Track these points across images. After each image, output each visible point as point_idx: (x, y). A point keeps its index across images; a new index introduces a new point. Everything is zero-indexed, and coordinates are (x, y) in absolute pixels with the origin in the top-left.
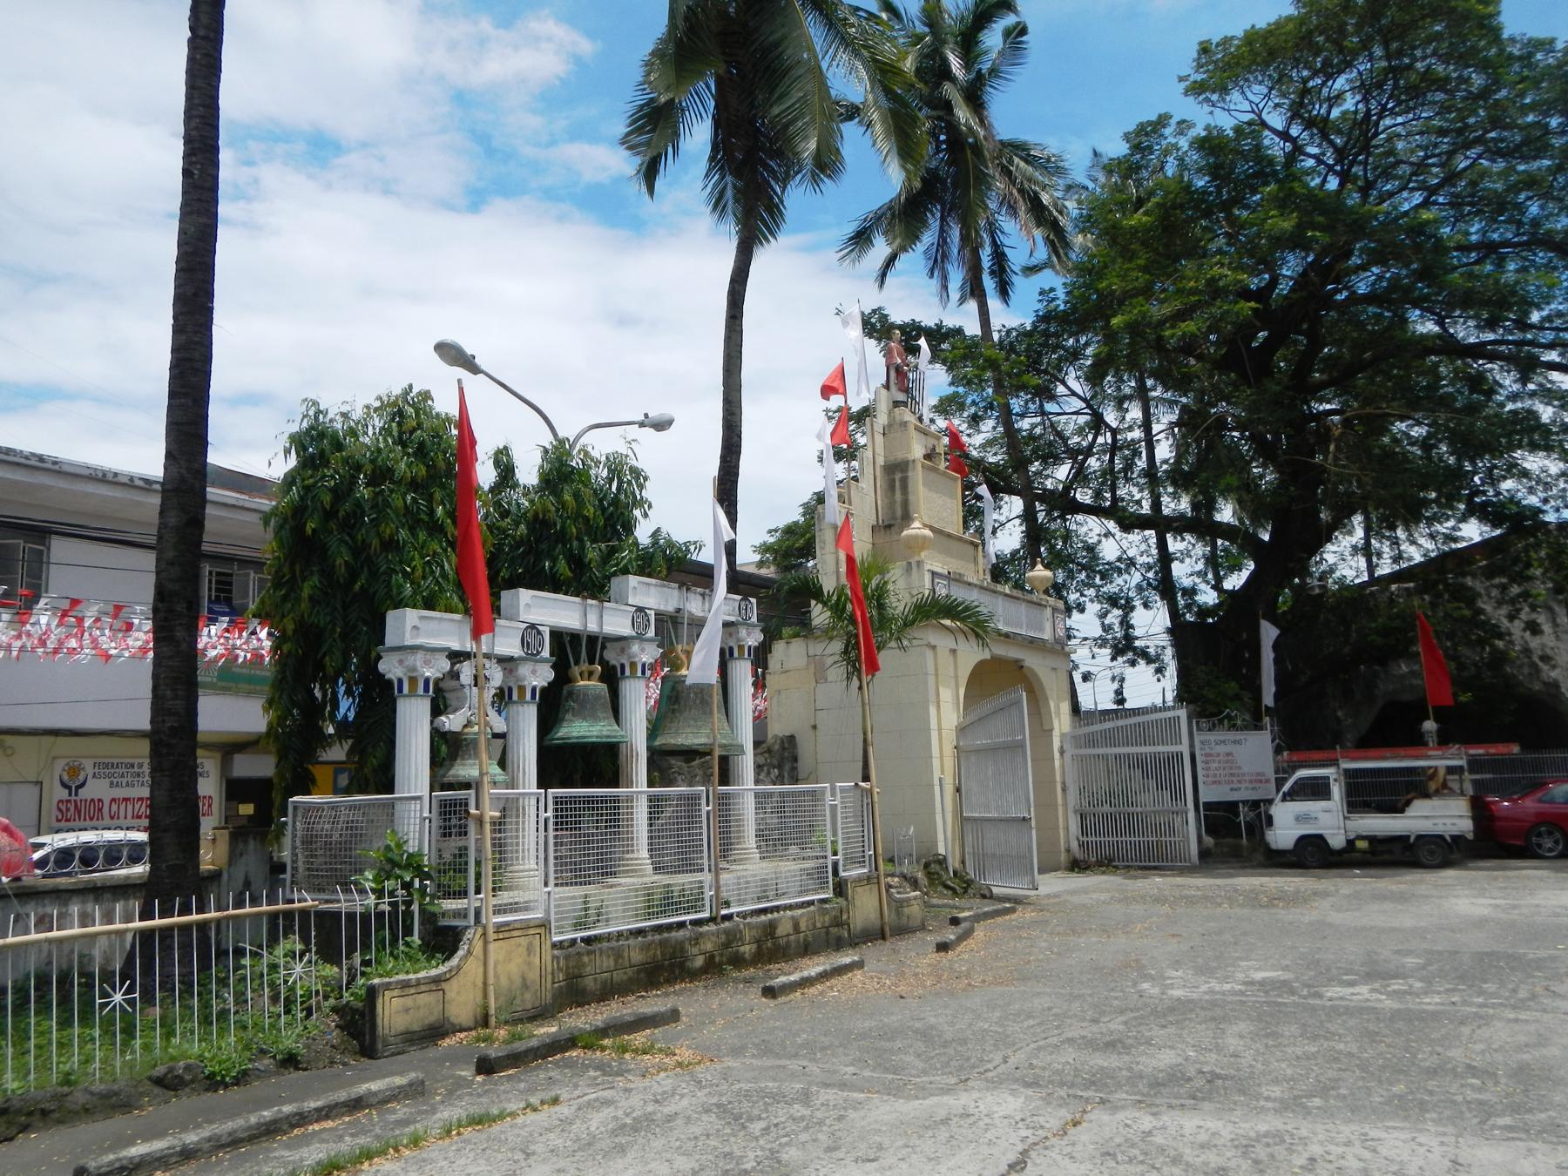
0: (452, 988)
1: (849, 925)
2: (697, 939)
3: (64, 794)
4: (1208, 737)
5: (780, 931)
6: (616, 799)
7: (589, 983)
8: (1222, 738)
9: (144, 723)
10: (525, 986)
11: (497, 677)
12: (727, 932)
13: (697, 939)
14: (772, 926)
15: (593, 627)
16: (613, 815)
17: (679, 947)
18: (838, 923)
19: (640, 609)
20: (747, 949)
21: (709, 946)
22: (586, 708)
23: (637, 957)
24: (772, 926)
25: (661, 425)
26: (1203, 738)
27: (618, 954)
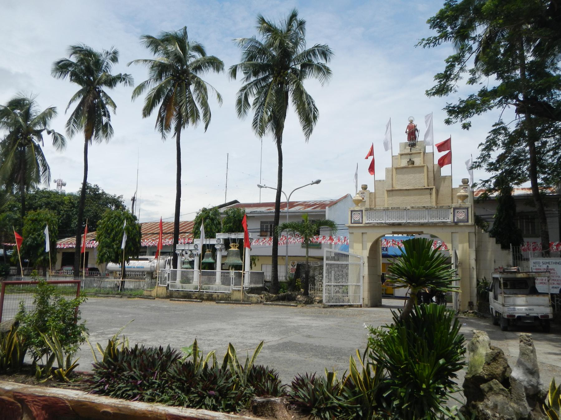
0: (152, 292)
1: (231, 298)
2: (194, 294)
3: (292, 267)
4: (538, 261)
5: (213, 296)
6: (214, 272)
7: (174, 296)
8: (547, 261)
9: (271, 254)
10: (162, 294)
11: (189, 253)
12: (201, 294)
13: (194, 294)
14: (212, 295)
15: (208, 243)
16: (214, 274)
17: (190, 294)
18: (229, 297)
19: (219, 239)
20: (205, 298)
21: (196, 295)
22: (208, 257)
23: (182, 294)
24: (212, 295)
25: (318, 182)
26: (535, 261)
27: (179, 293)
